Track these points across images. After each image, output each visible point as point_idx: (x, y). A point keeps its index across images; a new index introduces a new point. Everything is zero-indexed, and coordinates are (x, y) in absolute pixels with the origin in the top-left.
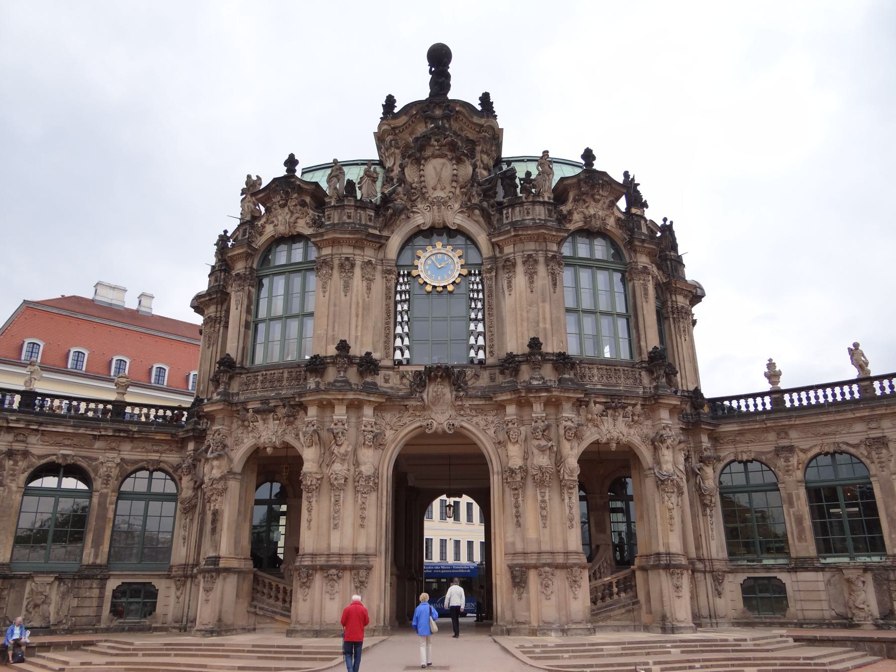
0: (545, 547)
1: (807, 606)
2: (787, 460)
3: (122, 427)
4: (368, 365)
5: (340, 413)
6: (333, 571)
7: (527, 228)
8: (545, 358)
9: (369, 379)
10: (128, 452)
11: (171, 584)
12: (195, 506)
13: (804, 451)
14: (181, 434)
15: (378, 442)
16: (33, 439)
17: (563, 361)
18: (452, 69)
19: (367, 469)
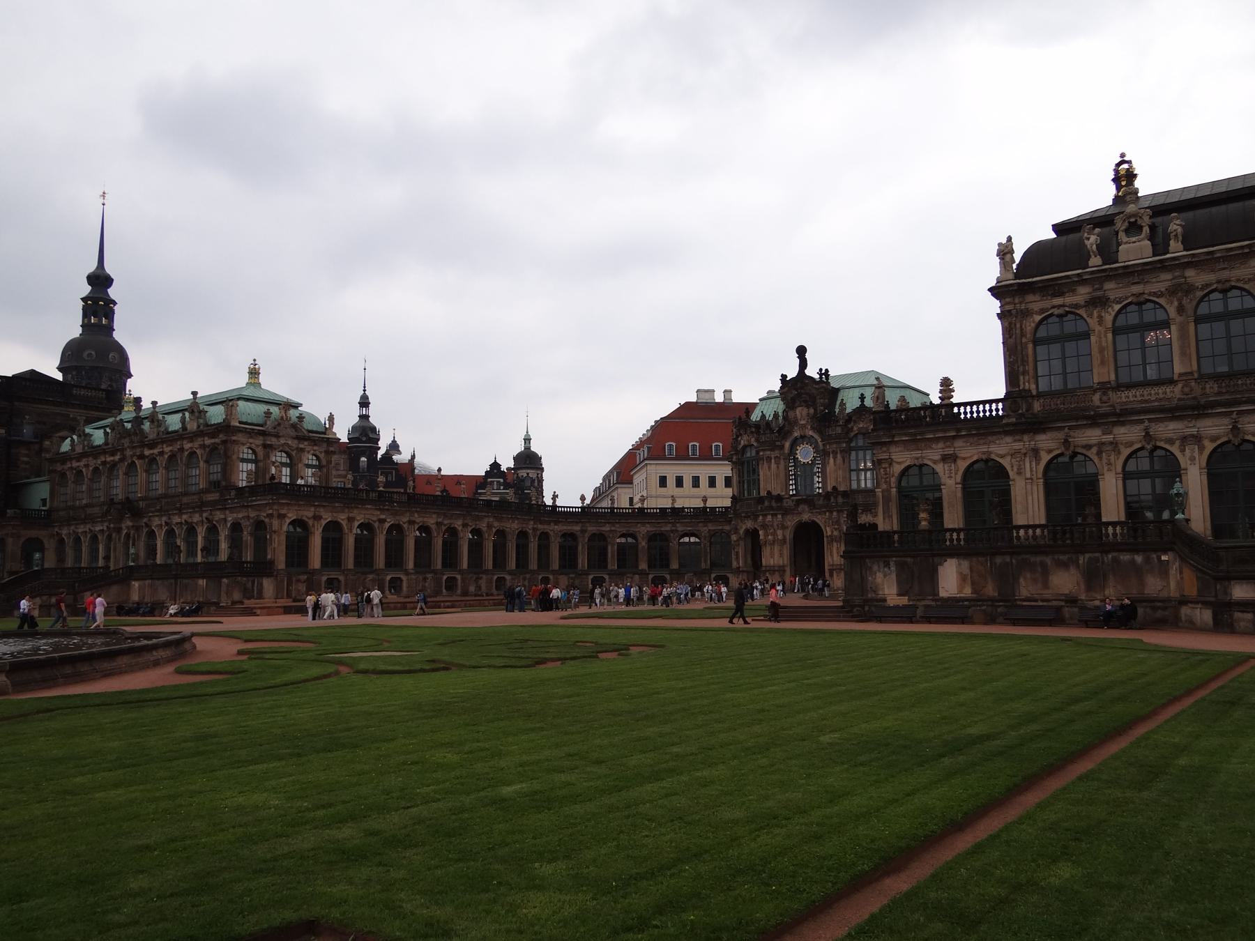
0: (839, 563)
4: (779, 498)
6: (771, 572)
9: (779, 505)
10: (711, 527)
15: (784, 528)
16: (678, 525)
17: (845, 494)
18: (807, 356)
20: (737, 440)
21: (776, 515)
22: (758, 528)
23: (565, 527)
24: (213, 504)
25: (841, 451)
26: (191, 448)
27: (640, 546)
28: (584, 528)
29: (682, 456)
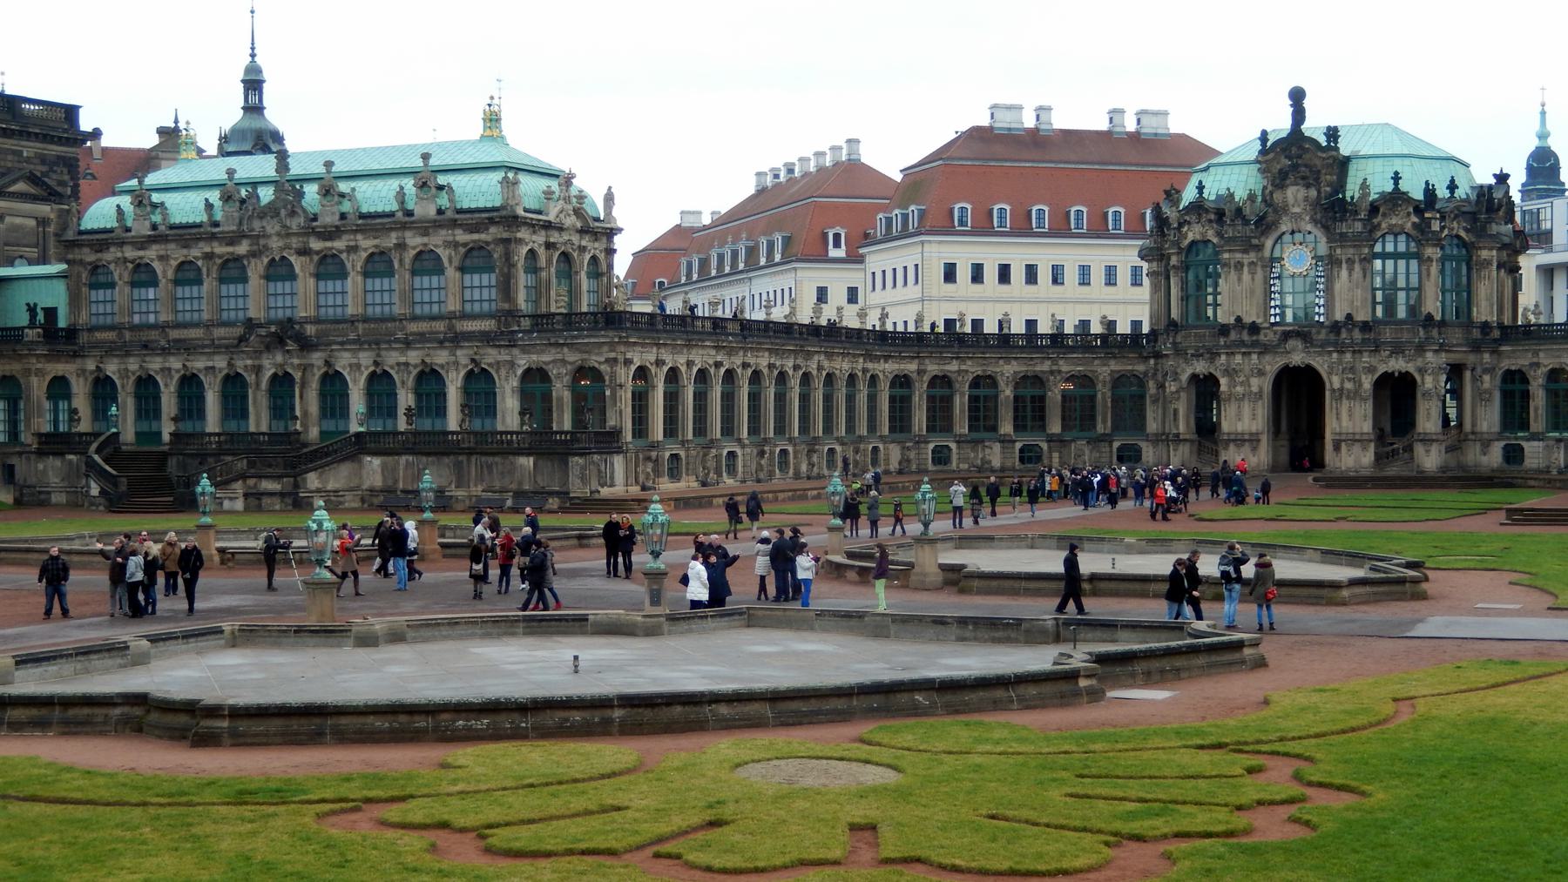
0: (1351, 431)
1: (1533, 461)
2: (1535, 371)
3: (1109, 351)
4: (1254, 328)
5: (1238, 359)
7: (1346, 241)
8: (1355, 324)
9: (1254, 338)
10: (1114, 366)
11: (1149, 444)
12: (1158, 399)
13: (1545, 366)
14: (1145, 354)
15: (1261, 373)
16: (1061, 362)
17: (1365, 327)
18: (1307, 103)
19: (1255, 389)
20: (1180, 232)
21: (1250, 353)
22: (1218, 374)
23: (896, 366)
24: (487, 338)
25: (1361, 261)
26: (425, 245)
27: (1002, 397)
28: (922, 367)
29: (984, 228)
